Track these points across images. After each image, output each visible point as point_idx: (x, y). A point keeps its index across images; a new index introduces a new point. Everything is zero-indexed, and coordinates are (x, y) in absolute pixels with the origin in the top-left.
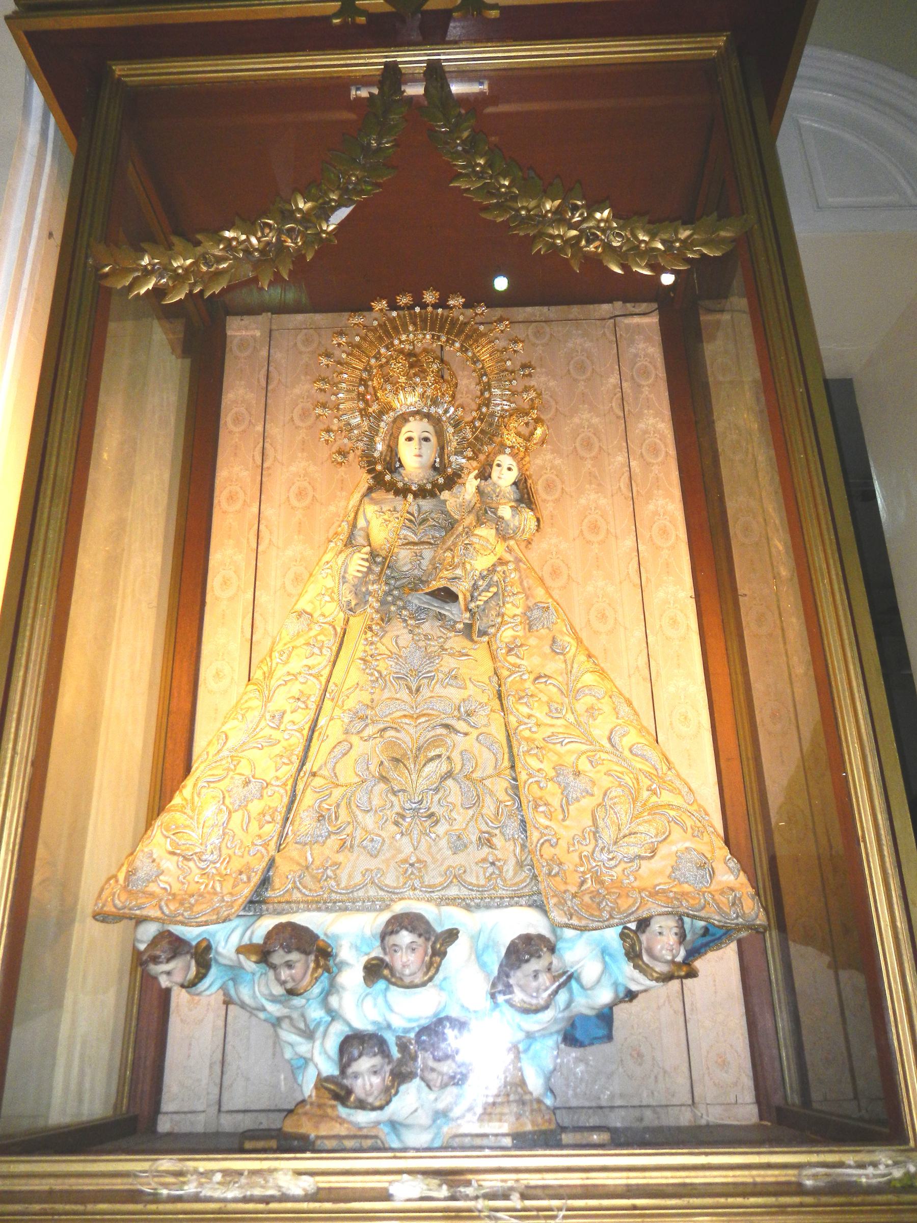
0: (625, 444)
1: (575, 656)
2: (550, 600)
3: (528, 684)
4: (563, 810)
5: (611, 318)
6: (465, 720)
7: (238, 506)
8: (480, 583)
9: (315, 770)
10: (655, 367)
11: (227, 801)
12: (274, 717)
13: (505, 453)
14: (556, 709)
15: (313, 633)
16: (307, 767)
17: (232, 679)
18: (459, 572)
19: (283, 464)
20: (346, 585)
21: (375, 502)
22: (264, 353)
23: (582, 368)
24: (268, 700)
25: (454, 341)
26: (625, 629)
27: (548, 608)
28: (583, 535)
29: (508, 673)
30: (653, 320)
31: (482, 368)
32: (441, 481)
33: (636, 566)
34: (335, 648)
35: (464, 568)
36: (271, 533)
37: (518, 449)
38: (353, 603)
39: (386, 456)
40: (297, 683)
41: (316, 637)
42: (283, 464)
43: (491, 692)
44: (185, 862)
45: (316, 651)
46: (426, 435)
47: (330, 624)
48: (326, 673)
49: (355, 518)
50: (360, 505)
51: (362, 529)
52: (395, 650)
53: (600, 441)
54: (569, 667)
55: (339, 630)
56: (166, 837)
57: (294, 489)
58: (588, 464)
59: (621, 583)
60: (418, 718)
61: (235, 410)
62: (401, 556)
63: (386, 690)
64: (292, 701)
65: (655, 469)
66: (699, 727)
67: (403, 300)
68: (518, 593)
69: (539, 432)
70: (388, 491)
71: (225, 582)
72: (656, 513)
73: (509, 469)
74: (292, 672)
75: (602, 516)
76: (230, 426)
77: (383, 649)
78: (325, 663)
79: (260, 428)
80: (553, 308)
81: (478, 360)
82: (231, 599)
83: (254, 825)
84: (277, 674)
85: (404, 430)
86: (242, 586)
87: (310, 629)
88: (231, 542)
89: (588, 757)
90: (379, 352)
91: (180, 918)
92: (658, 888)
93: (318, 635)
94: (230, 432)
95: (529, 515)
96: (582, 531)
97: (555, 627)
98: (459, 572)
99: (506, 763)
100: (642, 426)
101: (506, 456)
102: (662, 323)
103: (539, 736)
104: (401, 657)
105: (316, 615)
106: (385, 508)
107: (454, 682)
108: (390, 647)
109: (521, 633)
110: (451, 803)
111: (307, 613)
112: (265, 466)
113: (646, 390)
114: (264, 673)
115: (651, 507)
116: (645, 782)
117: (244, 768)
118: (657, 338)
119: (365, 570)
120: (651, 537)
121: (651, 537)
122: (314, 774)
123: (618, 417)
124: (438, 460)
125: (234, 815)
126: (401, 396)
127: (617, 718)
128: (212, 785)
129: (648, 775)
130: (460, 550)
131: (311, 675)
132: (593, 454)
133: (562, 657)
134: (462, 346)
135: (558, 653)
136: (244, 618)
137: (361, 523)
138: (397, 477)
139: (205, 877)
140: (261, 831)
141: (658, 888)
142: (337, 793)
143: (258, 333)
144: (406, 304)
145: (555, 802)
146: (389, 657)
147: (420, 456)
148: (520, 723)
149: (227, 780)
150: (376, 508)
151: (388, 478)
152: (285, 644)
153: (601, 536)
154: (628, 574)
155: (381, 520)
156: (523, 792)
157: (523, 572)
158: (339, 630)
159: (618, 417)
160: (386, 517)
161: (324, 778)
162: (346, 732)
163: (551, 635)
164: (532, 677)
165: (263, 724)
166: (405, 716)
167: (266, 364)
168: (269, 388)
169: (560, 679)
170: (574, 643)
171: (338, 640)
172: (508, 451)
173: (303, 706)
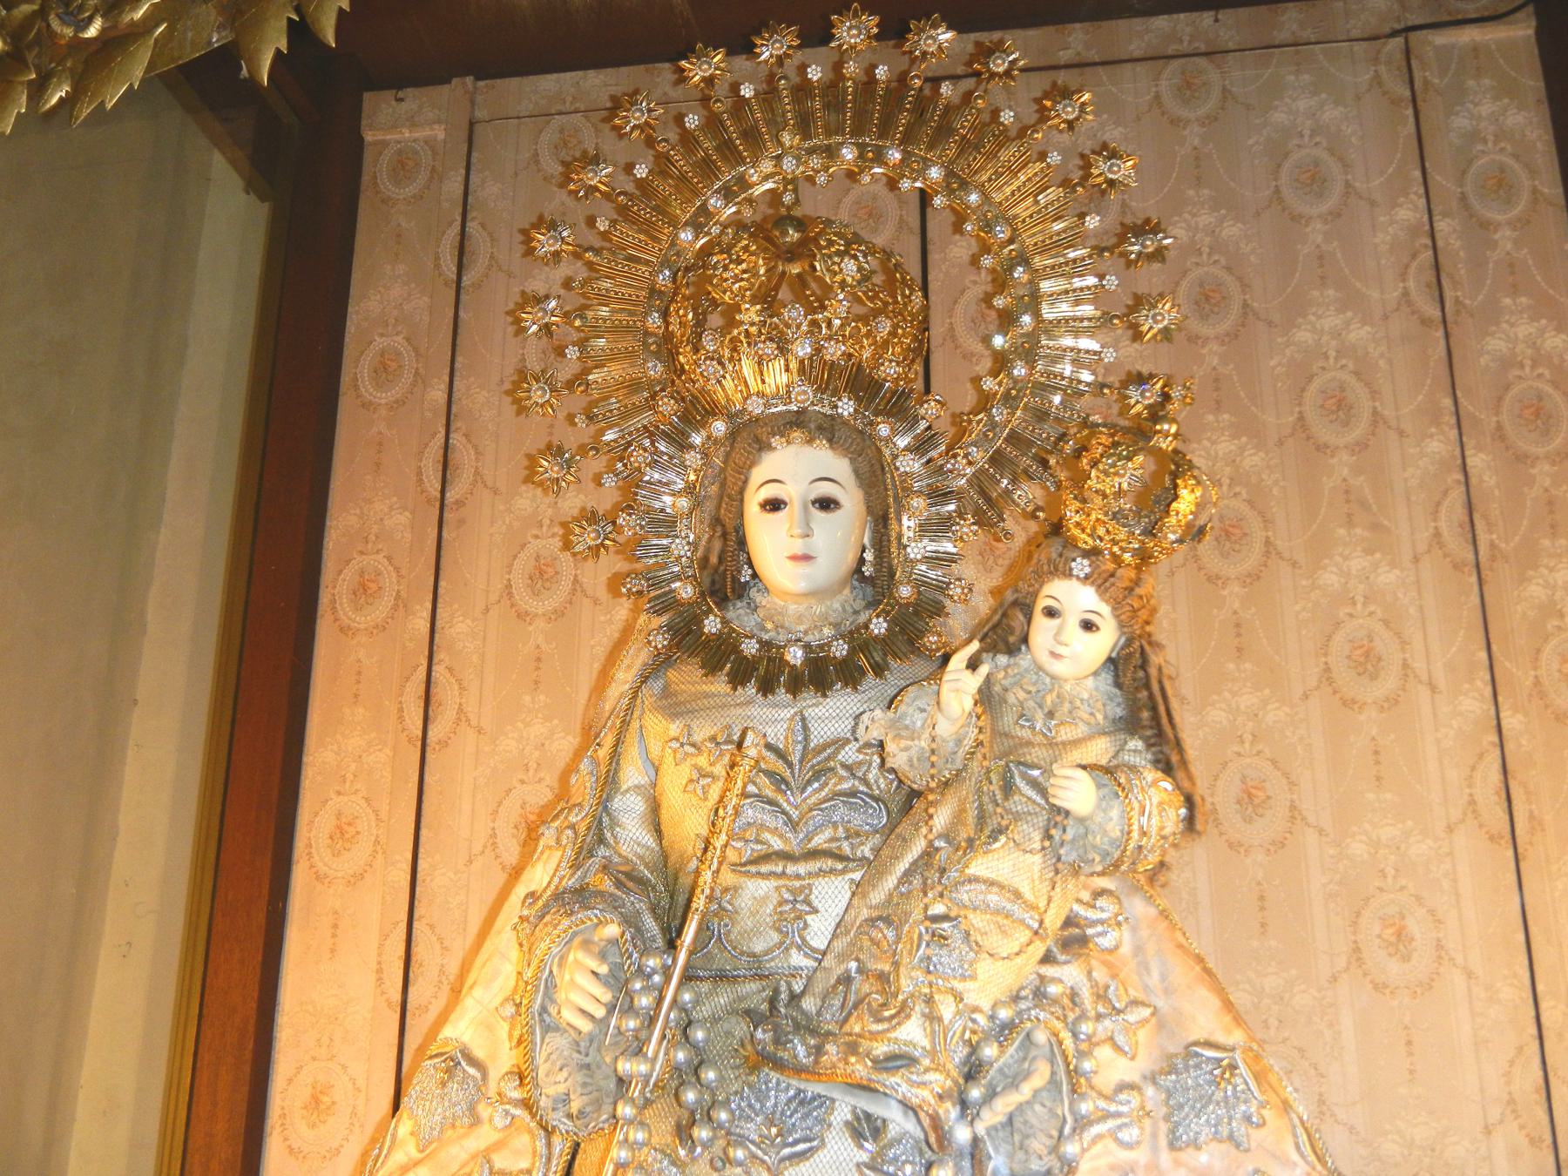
0: (1447, 402)
5: (1394, 33)
7: (380, 610)
10: (1532, 172)
13: (1068, 574)
15: (484, 1137)
17: (354, 1113)
18: (912, 1032)
19: (496, 492)
20: (557, 1042)
21: (673, 706)
22: (454, 186)
23: (1314, 181)
26: (1470, 975)
27: (1233, 1067)
28: (1330, 681)
30: (1522, 31)
32: (879, 627)
33: (1495, 776)
35: (932, 1018)
36: (462, 689)
37: (1117, 559)
38: (575, 1106)
39: (708, 550)
41: (486, 1155)
42: (496, 492)
46: (826, 489)
49: (615, 755)
50: (630, 709)
53: (1374, 394)
57: (524, 563)
58: (1342, 465)
61: (380, 342)
62: (745, 901)
68: (1135, 1003)
69: (1186, 502)
70: (712, 668)
71: (342, 834)
73: (1088, 626)
75: (1386, 623)
76: (368, 390)
79: (438, 394)
85: (758, 474)
87: (476, 1121)
90: (703, 209)
93: (498, 1146)
94: (366, 405)
97: (1256, 1135)
98: (912, 1032)
101: (1074, 581)
105: (494, 1075)
106: (701, 733)
111: (473, 1062)
112: (450, 496)
113: (1505, 238)
115: (1535, 590)
118: (1533, 83)
119: (600, 1012)
120: (1537, 682)
121: (1537, 682)
123: (1425, 322)
124: (869, 556)
126: (747, 368)
130: (916, 927)
137: (633, 774)
138: (739, 615)
143: (439, 133)
147: (806, 558)
150: (675, 728)
151: (712, 625)
153: (1389, 683)
155: (686, 771)
159: (1425, 322)
160: (702, 761)
168: (466, 281)
172: (1081, 566)
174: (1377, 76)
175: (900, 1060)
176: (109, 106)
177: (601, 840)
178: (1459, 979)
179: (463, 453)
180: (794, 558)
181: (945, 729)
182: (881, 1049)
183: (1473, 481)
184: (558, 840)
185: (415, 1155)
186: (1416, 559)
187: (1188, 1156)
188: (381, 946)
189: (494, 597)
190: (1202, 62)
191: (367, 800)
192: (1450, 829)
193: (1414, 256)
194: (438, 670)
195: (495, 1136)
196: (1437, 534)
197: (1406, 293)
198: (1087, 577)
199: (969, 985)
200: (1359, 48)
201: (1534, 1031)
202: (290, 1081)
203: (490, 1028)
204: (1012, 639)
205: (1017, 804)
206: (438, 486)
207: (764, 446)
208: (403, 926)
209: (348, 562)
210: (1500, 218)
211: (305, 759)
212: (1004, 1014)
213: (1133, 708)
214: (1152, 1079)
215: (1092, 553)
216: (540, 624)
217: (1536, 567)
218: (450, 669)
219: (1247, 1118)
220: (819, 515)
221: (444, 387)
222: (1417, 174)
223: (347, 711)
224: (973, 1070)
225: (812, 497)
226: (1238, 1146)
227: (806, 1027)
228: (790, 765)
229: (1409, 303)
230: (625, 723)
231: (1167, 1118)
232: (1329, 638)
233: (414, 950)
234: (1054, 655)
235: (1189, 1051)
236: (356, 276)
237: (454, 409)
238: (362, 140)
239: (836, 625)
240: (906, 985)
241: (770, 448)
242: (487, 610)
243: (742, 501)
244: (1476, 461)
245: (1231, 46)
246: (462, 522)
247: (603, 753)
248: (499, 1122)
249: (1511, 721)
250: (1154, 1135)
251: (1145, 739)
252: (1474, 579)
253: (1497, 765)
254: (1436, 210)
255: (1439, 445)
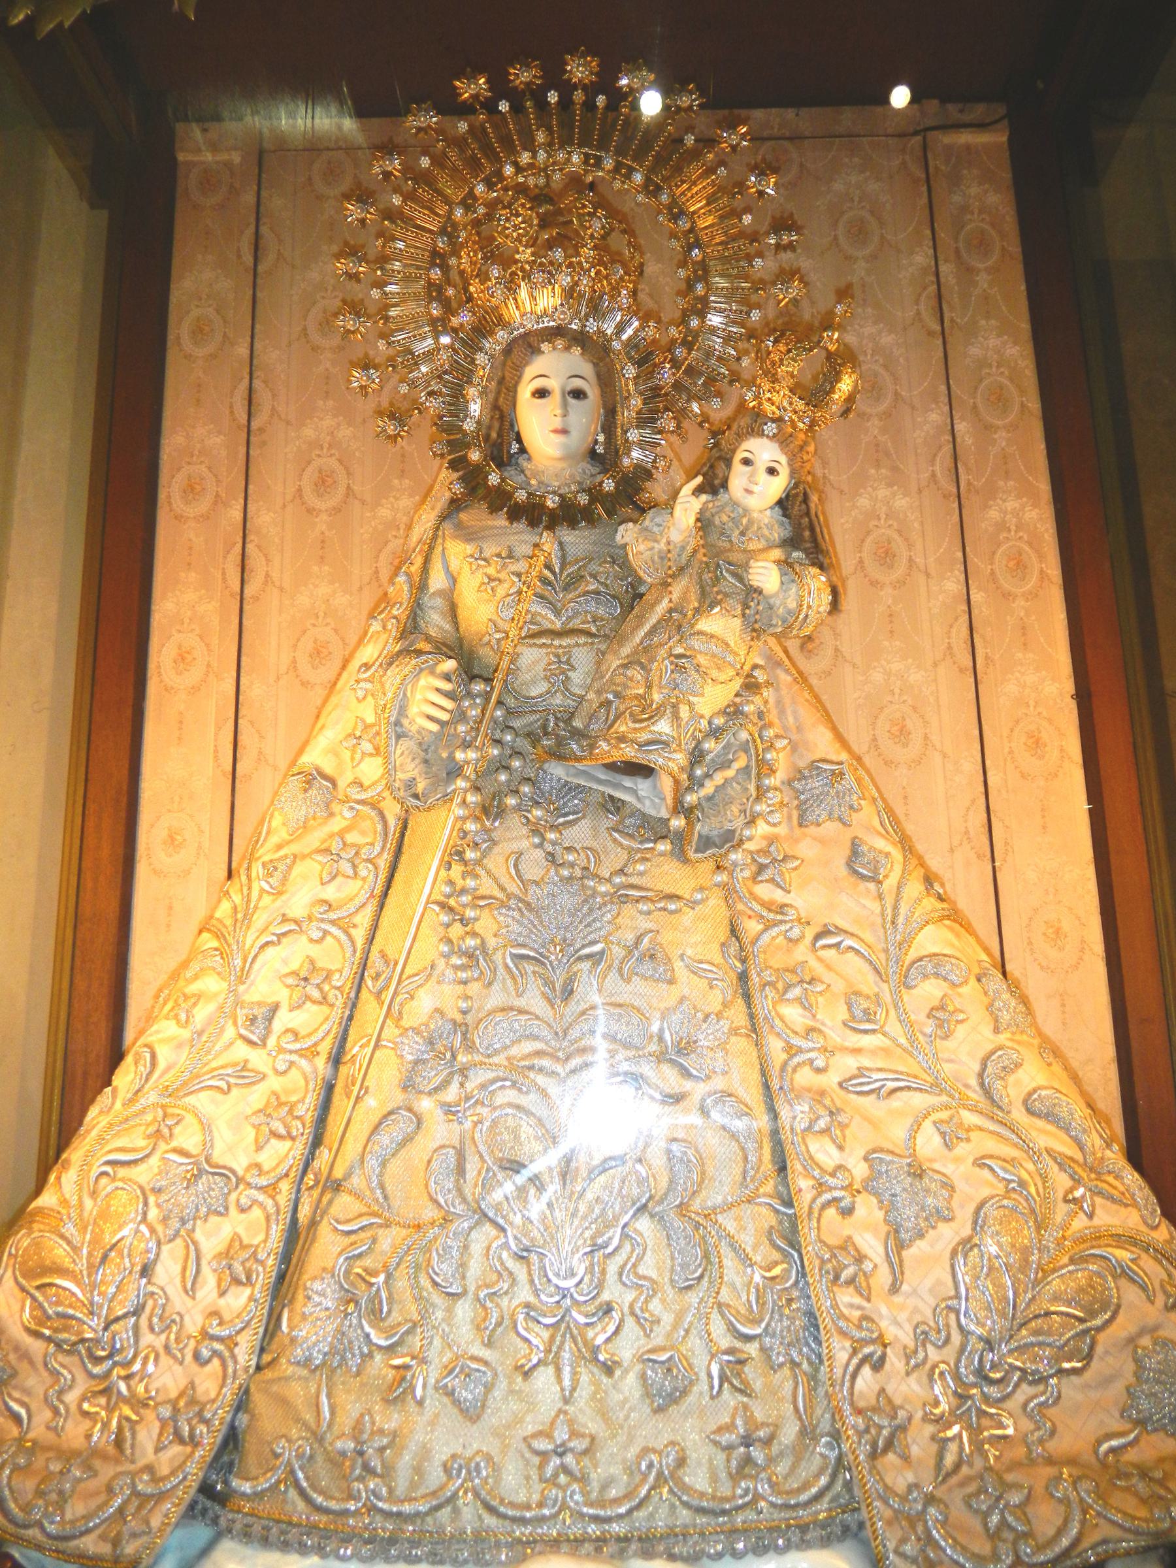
0: (943, 388)
1: (899, 887)
2: (844, 756)
3: (802, 952)
4: (891, 1264)
5: (916, 133)
6: (671, 1061)
7: (203, 505)
8: (709, 745)
9: (338, 1173)
11: (153, 1213)
12: (253, 1020)
13: (762, 434)
14: (866, 1012)
15: (337, 824)
16: (324, 1156)
17: (200, 847)
18: (663, 727)
20: (405, 744)
21: (468, 535)
22: (249, 198)
24: (243, 976)
25: (631, 170)
26: (945, 756)
27: (842, 774)
29: (761, 927)
31: (692, 230)
32: (609, 485)
34: (384, 862)
35: (676, 716)
36: (268, 560)
39: (490, 428)
40: (304, 938)
41: (341, 834)
43: (726, 986)
44: (60, 1357)
45: (346, 867)
46: (578, 383)
47: (374, 806)
48: (364, 920)
50: (435, 537)
51: (439, 593)
52: (513, 887)
54: (889, 911)
55: (392, 822)
56: (23, 1289)
57: (310, 474)
58: (874, 427)
59: (935, 665)
60: (567, 1059)
63: (496, 986)
64: (290, 981)
65: (1001, 437)
66: (1082, 950)
67: (523, 76)
69: (846, 385)
70: (494, 509)
71: (183, 659)
72: (1002, 526)
73: (772, 471)
74: (291, 915)
77: (487, 886)
78: (362, 898)
79: (243, 351)
80: (804, 112)
81: (682, 213)
82: (195, 690)
83: (209, 1280)
84: (260, 920)
85: (530, 371)
86: (215, 664)
87: (332, 815)
88: (193, 576)
89: (935, 1123)
90: (471, 194)
91: (33, 1533)
92: (1105, 1447)
93: (348, 829)
94: (188, 357)
95: (816, 582)
96: (861, 561)
98: (663, 727)
99: (768, 1166)
100: (975, 351)
101: (765, 440)
102: (1010, 139)
103: (831, 1080)
104: (528, 905)
105: (341, 784)
106: (490, 550)
107: (647, 968)
108: (504, 880)
109: (782, 830)
110: (645, 1278)
112: (255, 425)
113: (983, 280)
114: (235, 908)
115: (994, 514)
116: (1062, 1181)
117: (188, 1137)
120: (993, 573)
122: (337, 1187)
123: (930, 333)
124: (601, 438)
125: (165, 1248)
126: (523, 293)
127: (996, 1030)
128: (122, 1172)
129: (1063, 1163)
130: (662, 666)
131: (333, 922)
132: (883, 407)
133: (872, 886)
134: (648, 180)
135: (863, 877)
136: (218, 728)
137: (437, 581)
139: (103, 1401)
140: (222, 1302)
141: (1105, 1447)
142: (387, 1240)
144: (528, 84)
145: (872, 1246)
146: (503, 905)
147: (564, 431)
148: (791, 1050)
149: (154, 1161)
150: (469, 549)
151: (494, 479)
152: (279, 847)
153: (900, 571)
154: (950, 648)
155: (479, 577)
156: (808, 1234)
157: (784, 692)
158: (392, 822)
159: (930, 333)
160: (491, 571)
161: (358, 1196)
162: (408, 1085)
163: (848, 834)
164: (810, 934)
165: (230, 1032)
166: (539, 1053)
167: (252, 220)
168: (260, 268)
169: (868, 936)
170: (897, 855)
171: (391, 844)
172: (770, 429)
173: (316, 994)
174: (904, 163)
175: (661, 743)
176: (67, 24)
177: (416, 626)
178: (937, 758)
179: (263, 396)
180: (555, 431)
181: (676, 536)
182: (644, 737)
183: (958, 440)
184: (384, 627)
185: (287, 837)
186: (920, 491)
187: (812, 830)
188: (216, 734)
189: (289, 497)
190: (786, 143)
191: (201, 637)
192: (935, 665)
193: (925, 289)
194: (249, 546)
195: (344, 824)
196: (934, 475)
197: (918, 313)
198: (775, 436)
199: (700, 699)
200: (891, 141)
201: (982, 789)
202: (152, 826)
203: (336, 754)
204: (717, 482)
205: (723, 586)
206: (245, 417)
207: (536, 351)
208: (232, 721)
209: (179, 469)
210: (981, 266)
211: (153, 607)
212: (719, 721)
213: (797, 528)
214: (789, 782)
215: (778, 420)
216: (324, 517)
217: (995, 499)
218: (259, 547)
219: (851, 807)
220: (572, 401)
221: (247, 345)
222: (928, 232)
223: (183, 575)
224: (697, 756)
225: (568, 389)
226: (844, 824)
227: (577, 734)
228: (554, 573)
229: (920, 320)
230: (431, 548)
231: (798, 807)
232: (863, 541)
233: (240, 738)
234: (749, 492)
235: (813, 766)
236: (176, 262)
237: (255, 362)
238: (175, 159)
239: (580, 483)
240: (657, 697)
241: (540, 352)
242: (284, 506)
243: (516, 392)
244: (960, 427)
245: (807, 133)
246: (264, 443)
247: (415, 568)
248: (348, 814)
249: (976, 597)
250: (790, 817)
251: (805, 551)
252: (956, 505)
253: (966, 624)
254: (941, 257)
255: (936, 416)
